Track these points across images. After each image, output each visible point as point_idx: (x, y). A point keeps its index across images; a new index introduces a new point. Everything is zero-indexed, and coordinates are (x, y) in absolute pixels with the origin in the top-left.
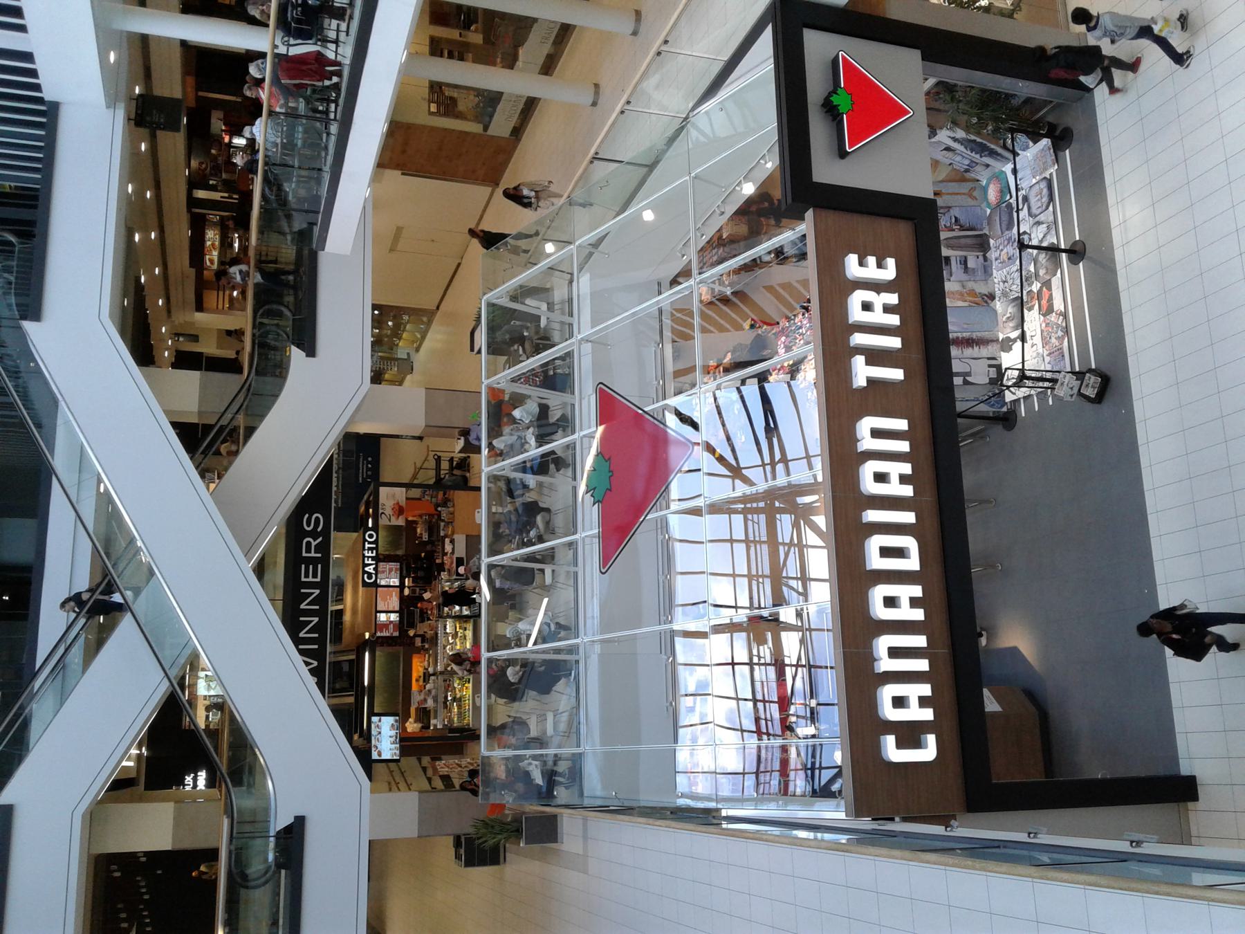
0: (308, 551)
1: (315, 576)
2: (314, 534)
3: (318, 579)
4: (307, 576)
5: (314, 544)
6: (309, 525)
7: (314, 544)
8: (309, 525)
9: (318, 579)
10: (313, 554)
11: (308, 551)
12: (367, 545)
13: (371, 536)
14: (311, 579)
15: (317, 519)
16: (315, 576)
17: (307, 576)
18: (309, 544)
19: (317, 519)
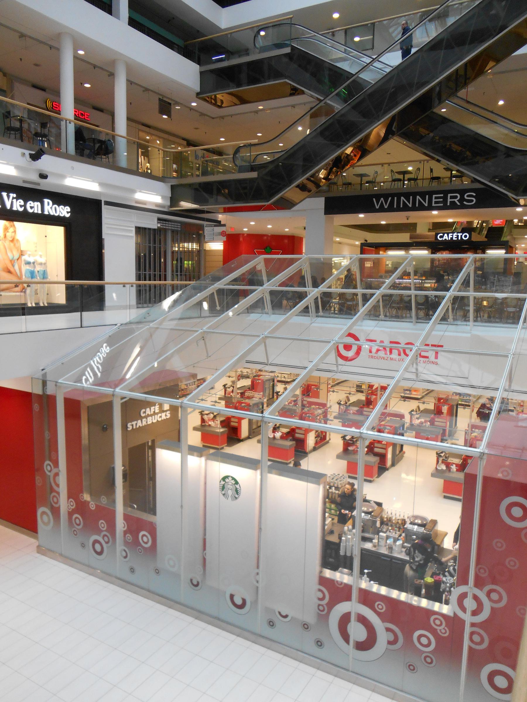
0: (452, 197)
1: (436, 203)
2: (462, 200)
3: (433, 205)
4: (436, 198)
5: (456, 200)
6: (468, 196)
7: (456, 200)
8: (467, 196)
9: (433, 205)
10: (449, 200)
11: (452, 197)
12: (460, 235)
13: (466, 236)
14: (434, 200)
15: (472, 201)
16: (436, 203)
17: (436, 198)
18: (456, 197)
19: (472, 201)
